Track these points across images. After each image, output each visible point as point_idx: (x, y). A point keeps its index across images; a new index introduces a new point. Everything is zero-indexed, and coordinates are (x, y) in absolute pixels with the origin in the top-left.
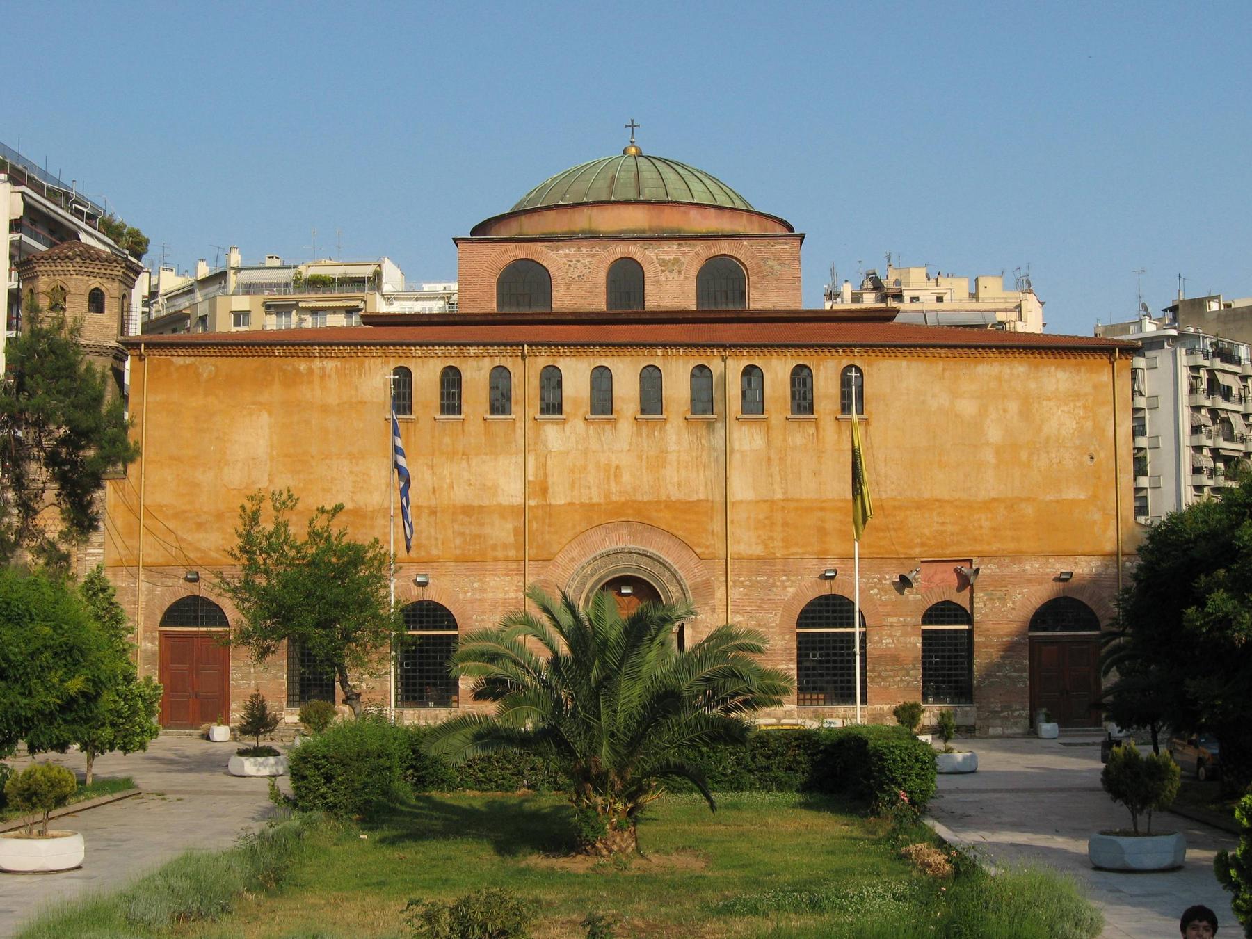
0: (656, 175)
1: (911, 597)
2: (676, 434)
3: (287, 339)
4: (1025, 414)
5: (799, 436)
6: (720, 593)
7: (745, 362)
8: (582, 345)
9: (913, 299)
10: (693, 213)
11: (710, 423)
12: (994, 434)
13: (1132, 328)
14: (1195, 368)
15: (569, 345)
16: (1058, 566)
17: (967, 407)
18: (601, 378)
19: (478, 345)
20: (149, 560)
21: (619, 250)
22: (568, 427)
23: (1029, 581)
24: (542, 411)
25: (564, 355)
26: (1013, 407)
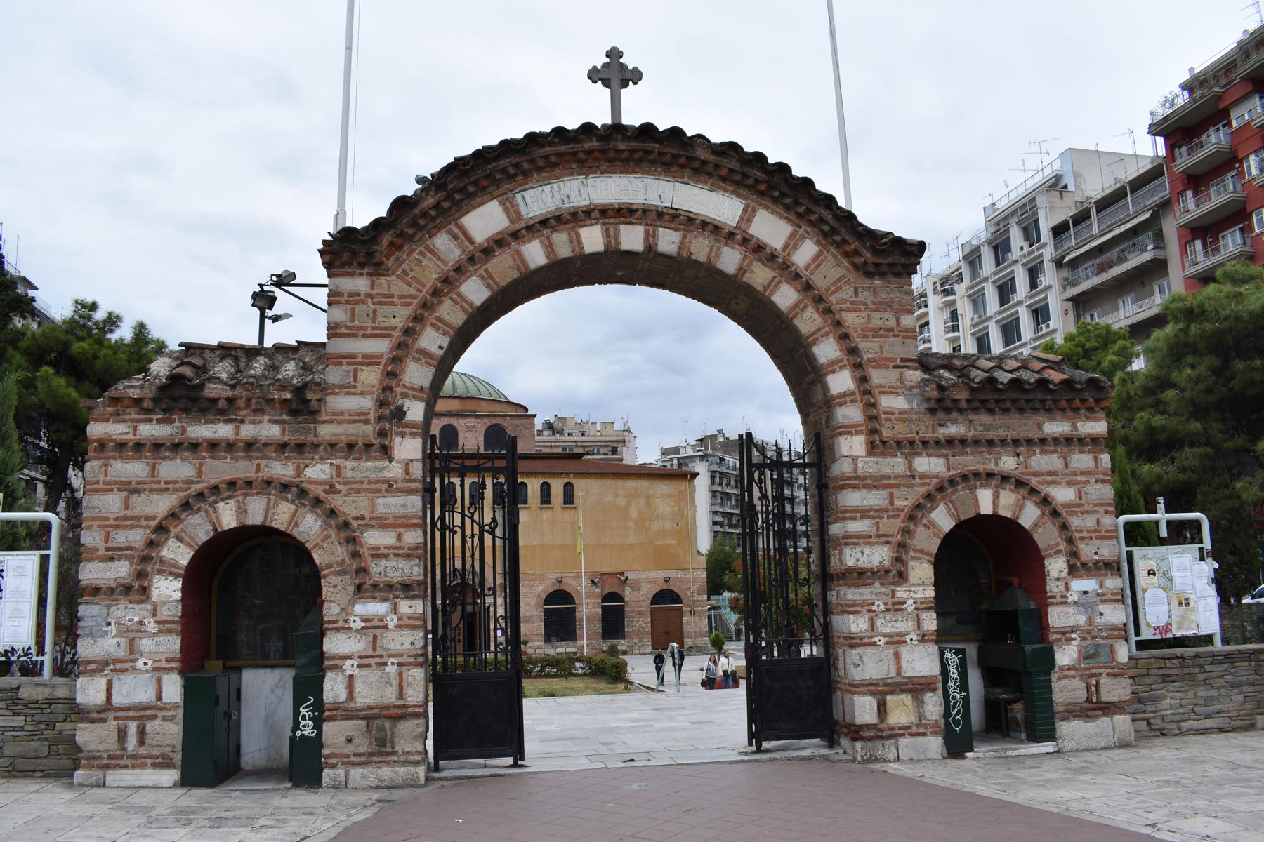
4: (648, 505)
5: (546, 515)
9: (570, 434)
10: (482, 403)
12: (634, 514)
14: (714, 472)
17: (622, 502)
26: (642, 501)
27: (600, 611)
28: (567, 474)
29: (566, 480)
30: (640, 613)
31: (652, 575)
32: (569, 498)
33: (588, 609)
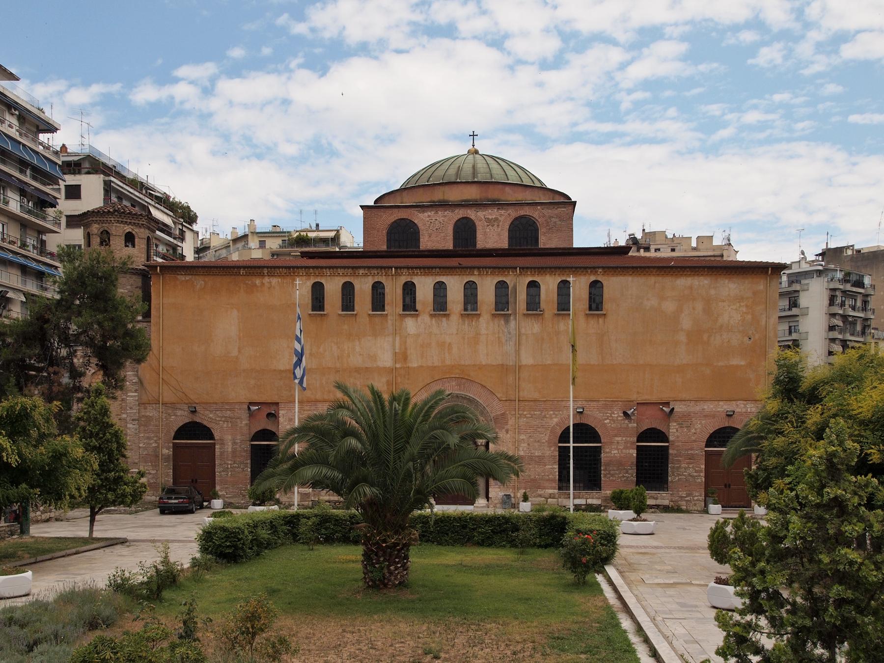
0: (485, 166)
1: (630, 425)
2: (485, 324)
3: (248, 264)
6: (511, 422)
7: (530, 279)
8: (428, 268)
11: (507, 317)
13: (793, 266)
14: (834, 290)
15: (420, 268)
16: (725, 407)
18: (440, 289)
19: (364, 268)
20: (166, 400)
21: (460, 213)
22: (419, 319)
23: (705, 416)
24: (404, 310)
25: (417, 275)
27: (634, 453)
28: (593, 269)
29: (593, 278)
30: (691, 458)
31: (708, 407)
32: (595, 302)
33: (619, 451)
